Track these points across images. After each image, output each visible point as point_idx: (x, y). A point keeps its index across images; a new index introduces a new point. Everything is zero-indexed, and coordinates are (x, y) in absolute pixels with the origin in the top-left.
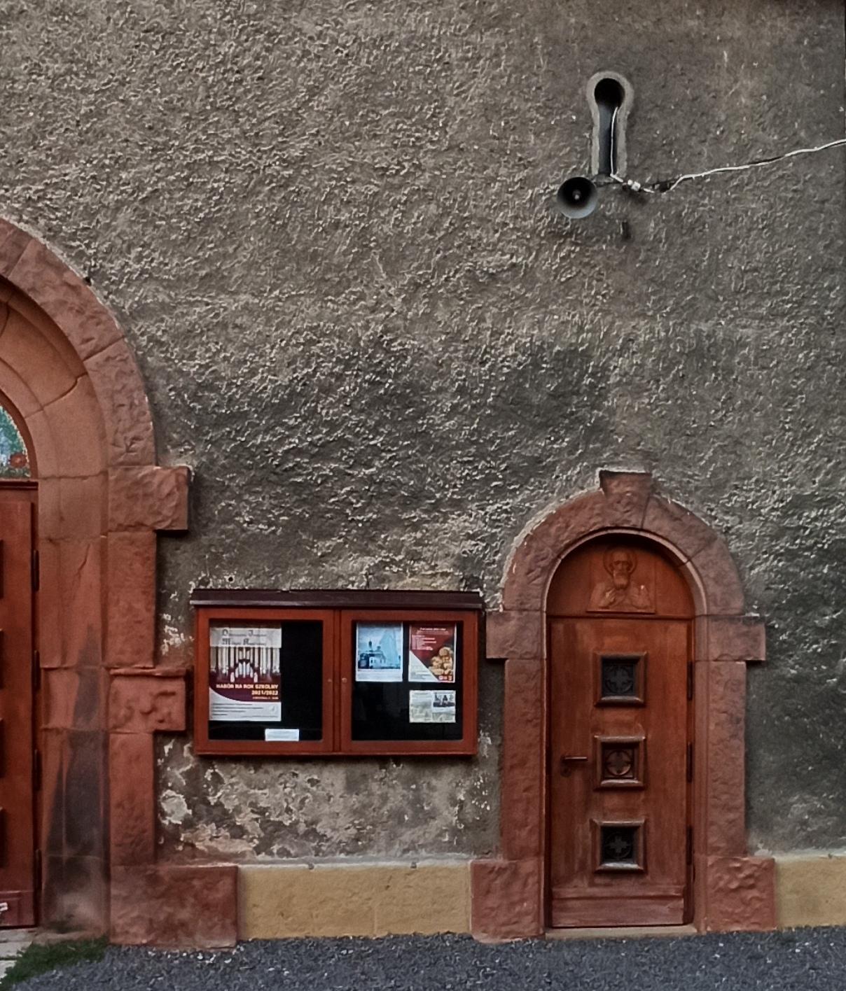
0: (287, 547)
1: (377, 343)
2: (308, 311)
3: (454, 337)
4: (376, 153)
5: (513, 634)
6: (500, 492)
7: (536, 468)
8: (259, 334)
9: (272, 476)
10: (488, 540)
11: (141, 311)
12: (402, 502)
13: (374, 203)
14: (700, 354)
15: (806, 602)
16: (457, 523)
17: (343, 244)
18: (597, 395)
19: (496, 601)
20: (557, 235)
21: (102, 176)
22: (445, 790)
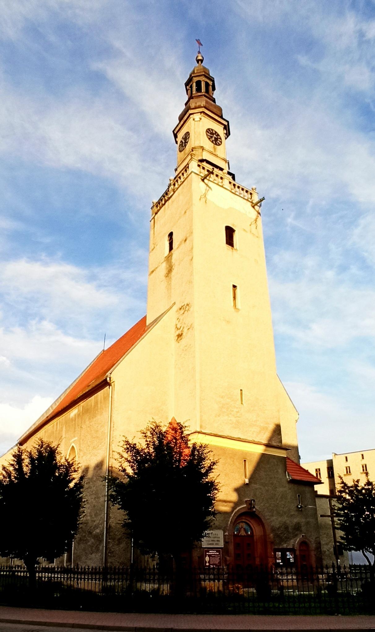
0: (280, 544)
2: (280, 519)
7: (296, 535)
8: (275, 521)
10: (295, 542)
12: (288, 539)
16: (292, 541)
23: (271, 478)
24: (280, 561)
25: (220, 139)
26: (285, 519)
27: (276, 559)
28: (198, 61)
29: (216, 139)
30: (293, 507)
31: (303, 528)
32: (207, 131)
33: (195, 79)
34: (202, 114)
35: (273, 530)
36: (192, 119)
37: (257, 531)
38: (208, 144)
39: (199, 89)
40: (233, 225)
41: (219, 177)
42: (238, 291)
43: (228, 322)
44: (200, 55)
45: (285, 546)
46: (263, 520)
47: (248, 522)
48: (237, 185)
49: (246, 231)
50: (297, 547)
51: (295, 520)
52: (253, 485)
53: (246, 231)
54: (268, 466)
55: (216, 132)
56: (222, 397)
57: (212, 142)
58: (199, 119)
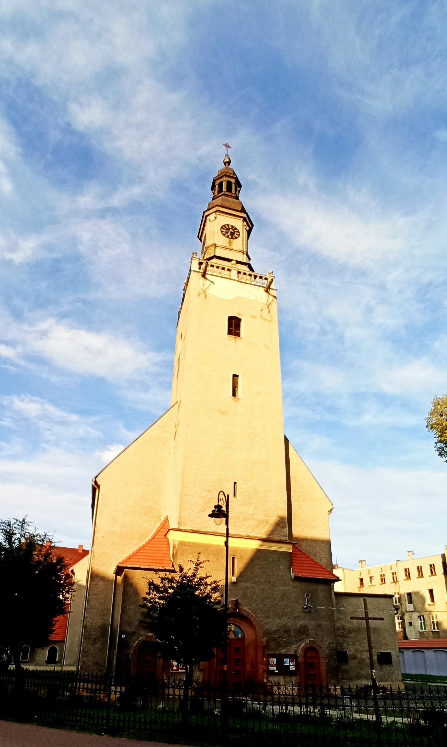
0: (276, 649)
1: (285, 625)
2: (278, 621)
3: (293, 624)
4: (284, 602)
5: (301, 660)
6: (298, 642)
7: (302, 640)
9: (275, 640)
11: (261, 621)
12: (288, 643)
13: (284, 608)
14: (319, 626)
15: (331, 656)
16: (294, 646)
17: (281, 613)
18: (308, 631)
19: (299, 655)
20: (303, 612)
21: (257, 606)
22: (294, 679)
23: (268, 576)
24: (275, 668)
25: (238, 232)
26: (285, 620)
27: (268, 665)
28: (225, 163)
29: (232, 234)
30: (298, 608)
31: (311, 632)
32: (222, 228)
33: (217, 182)
34: (217, 213)
35: (267, 633)
36: (208, 221)
37: (249, 635)
38: (222, 240)
39: (220, 190)
40: (239, 314)
41: (226, 269)
42: (240, 380)
43: (224, 413)
44: (227, 158)
45: (283, 651)
46: (253, 622)
47: (239, 624)
48: (258, 275)
49: (255, 318)
50: (300, 653)
51: (300, 623)
52: (242, 584)
53: (255, 318)
54: (266, 563)
55: (233, 227)
56: (209, 492)
57: (228, 237)
58: (214, 219)
